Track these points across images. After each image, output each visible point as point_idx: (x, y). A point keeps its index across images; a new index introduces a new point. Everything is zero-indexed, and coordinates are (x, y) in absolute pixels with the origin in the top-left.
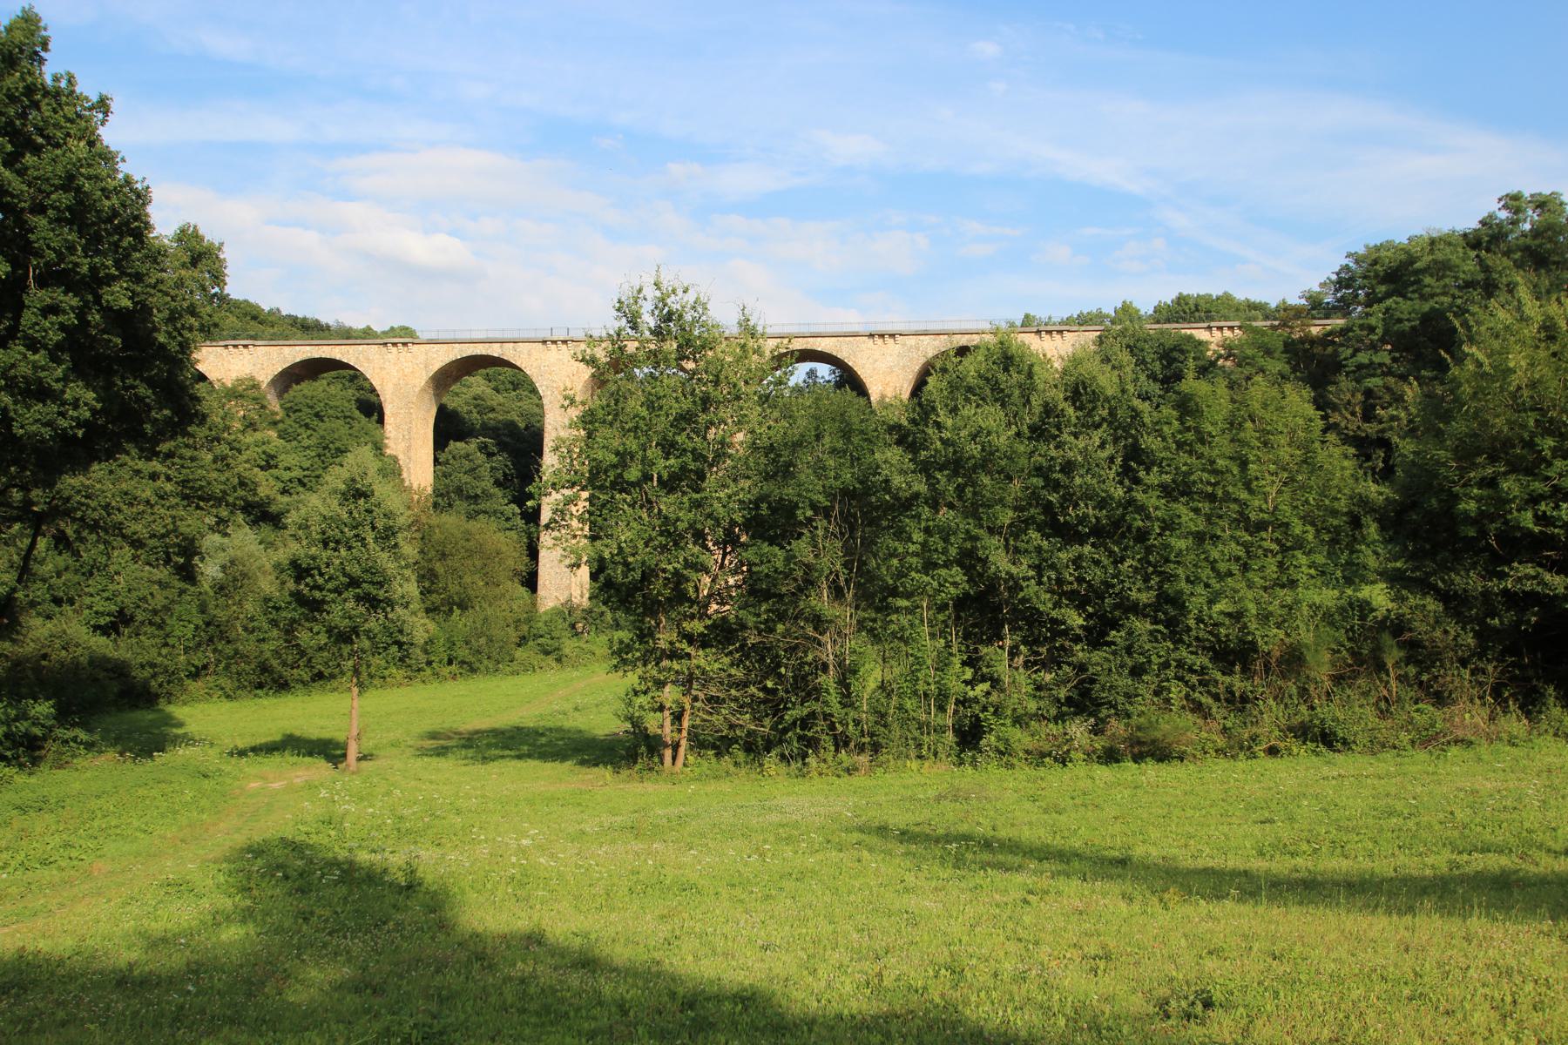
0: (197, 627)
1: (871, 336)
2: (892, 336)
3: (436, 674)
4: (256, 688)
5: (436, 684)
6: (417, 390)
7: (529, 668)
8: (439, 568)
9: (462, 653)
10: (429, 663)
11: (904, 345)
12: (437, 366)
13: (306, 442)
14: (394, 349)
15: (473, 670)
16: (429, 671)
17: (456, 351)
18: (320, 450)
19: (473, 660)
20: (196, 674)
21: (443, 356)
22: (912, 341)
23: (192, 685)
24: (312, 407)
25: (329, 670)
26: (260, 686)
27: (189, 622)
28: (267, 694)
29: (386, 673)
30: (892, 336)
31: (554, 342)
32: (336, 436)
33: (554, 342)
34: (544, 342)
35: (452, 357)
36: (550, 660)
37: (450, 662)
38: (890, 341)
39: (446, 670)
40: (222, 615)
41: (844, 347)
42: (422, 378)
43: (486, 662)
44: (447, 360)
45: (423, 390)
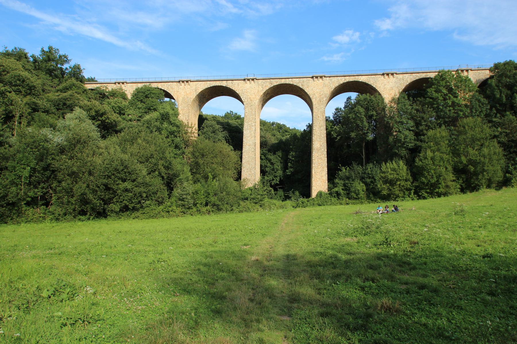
0: (34, 170)
1: (383, 74)
2: (392, 74)
3: (199, 211)
4: (82, 215)
5: (199, 216)
6: (192, 100)
7: (248, 210)
8: (201, 161)
9: (213, 199)
10: (195, 205)
11: (397, 78)
12: (200, 90)
13: (140, 106)
14: (183, 84)
15: (219, 209)
16: (195, 209)
18: (147, 110)
19: (220, 203)
20: (33, 203)
21: (202, 86)
22: (400, 76)
23: (30, 211)
24: (144, 93)
25: (133, 205)
26: (83, 213)
27: (28, 166)
28: (89, 219)
29: (170, 209)
30: (392, 74)
31: (249, 80)
32: (154, 104)
33: (249, 80)
34: (244, 80)
35: (206, 87)
36: (257, 206)
37: (206, 205)
39: (204, 209)
40: (56, 164)
42: (193, 95)
43: (226, 206)
45: (194, 100)
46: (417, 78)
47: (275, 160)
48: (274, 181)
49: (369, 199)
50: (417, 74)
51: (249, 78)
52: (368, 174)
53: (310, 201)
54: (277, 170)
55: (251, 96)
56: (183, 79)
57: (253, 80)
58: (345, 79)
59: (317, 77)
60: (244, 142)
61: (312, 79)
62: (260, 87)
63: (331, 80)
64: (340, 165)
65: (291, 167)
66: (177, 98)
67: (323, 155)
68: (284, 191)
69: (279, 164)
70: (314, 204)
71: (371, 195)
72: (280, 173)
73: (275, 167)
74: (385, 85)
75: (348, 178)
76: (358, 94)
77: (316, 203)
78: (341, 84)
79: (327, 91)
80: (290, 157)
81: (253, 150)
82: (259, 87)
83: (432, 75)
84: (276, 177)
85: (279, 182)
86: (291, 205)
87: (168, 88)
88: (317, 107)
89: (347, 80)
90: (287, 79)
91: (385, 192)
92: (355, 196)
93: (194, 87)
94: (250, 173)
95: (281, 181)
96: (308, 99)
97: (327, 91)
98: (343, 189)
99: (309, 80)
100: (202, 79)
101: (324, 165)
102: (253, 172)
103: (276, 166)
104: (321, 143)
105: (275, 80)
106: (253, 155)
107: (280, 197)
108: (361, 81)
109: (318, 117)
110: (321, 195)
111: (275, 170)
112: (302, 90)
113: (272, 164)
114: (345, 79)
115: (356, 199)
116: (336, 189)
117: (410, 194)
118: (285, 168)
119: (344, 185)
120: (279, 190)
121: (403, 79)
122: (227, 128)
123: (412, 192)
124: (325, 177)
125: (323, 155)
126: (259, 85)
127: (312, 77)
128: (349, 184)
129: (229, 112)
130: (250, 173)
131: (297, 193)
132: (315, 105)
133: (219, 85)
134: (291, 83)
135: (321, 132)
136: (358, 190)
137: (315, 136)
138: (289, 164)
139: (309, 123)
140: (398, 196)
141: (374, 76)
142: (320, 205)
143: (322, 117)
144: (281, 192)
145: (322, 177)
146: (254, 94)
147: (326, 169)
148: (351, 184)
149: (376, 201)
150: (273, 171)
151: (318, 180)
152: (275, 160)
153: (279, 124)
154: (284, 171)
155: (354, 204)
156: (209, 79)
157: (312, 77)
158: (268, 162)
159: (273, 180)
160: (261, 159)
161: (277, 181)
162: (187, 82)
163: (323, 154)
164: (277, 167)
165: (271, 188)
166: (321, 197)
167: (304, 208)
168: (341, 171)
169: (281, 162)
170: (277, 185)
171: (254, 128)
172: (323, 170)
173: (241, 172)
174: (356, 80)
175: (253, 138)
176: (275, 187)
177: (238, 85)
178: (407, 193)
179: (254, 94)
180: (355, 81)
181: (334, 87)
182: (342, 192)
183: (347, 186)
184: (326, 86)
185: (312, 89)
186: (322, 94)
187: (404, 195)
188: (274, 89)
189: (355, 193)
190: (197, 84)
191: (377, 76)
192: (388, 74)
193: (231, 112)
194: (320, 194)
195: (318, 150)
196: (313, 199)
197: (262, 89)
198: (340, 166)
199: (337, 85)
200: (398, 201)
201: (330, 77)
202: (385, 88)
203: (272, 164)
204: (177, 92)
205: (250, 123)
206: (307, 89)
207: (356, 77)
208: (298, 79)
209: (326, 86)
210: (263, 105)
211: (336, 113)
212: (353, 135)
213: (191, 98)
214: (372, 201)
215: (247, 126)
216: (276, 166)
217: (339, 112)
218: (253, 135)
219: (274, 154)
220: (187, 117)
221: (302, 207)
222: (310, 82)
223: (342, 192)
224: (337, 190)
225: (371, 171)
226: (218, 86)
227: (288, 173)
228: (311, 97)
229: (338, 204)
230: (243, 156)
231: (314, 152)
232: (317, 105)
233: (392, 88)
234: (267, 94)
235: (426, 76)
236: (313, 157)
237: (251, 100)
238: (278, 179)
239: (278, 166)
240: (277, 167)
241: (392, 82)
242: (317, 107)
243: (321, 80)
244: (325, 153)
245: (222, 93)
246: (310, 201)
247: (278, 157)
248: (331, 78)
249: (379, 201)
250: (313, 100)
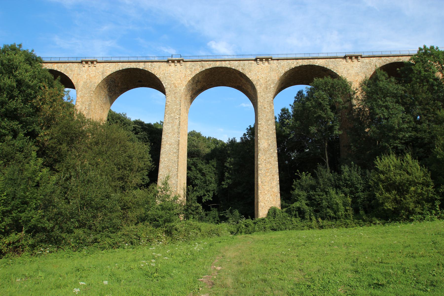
2: (357, 57)
6: (96, 85)
11: (363, 62)
12: (109, 73)
14: (86, 66)
22: (367, 60)
30: (357, 57)
34: (168, 62)
35: (117, 69)
36: (160, 233)
38: (355, 60)
41: (330, 63)
44: (114, 70)
46: (388, 62)
47: (207, 171)
48: (206, 197)
49: (358, 219)
50: (387, 58)
51: (174, 59)
52: (346, 180)
53: (259, 223)
54: (211, 183)
55: (175, 82)
56: (87, 59)
57: (179, 61)
58: (298, 63)
59: (261, 60)
60: (163, 140)
61: (255, 63)
62: (188, 70)
63: (279, 63)
64: (298, 171)
65: (228, 178)
66: (77, 82)
67: (273, 158)
68: (219, 211)
69: (212, 175)
70: (265, 228)
71: (362, 212)
72: (213, 186)
73: (207, 179)
74: (348, 70)
75: (313, 188)
77: (269, 225)
78: (293, 69)
79: (275, 76)
80: (227, 165)
81: (175, 151)
82: (186, 71)
83: (406, 59)
84: (208, 191)
85: (212, 198)
86: (228, 230)
87: (66, 70)
88: (262, 96)
89: (301, 64)
90: (223, 62)
91: (389, 206)
92: (332, 215)
93: (101, 70)
95: (214, 196)
96: (250, 90)
97: (275, 76)
98: (307, 204)
99: (251, 63)
100: (114, 59)
101: (274, 172)
103: (208, 178)
104: (270, 141)
105: (208, 62)
106: (176, 158)
107: (214, 218)
108: (317, 65)
109: (265, 108)
110: (275, 214)
111: (208, 183)
112: (242, 76)
113: (203, 175)
114: (298, 63)
115: (333, 218)
116: (297, 204)
117: (433, 207)
118: (221, 179)
119: (309, 198)
120: (212, 209)
121: (370, 64)
122: (147, 128)
123: (437, 203)
124: (276, 189)
125: (273, 158)
126: (186, 68)
127: (256, 60)
128: (317, 196)
129: (159, 123)
131: (237, 212)
132: (260, 93)
133: (135, 67)
134: (229, 66)
135: (269, 127)
136: (337, 204)
137: (261, 133)
138: (226, 174)
139: (250, 126)
140: (412, 213)
141: (334, 60)
142: (274, 230)
143: (269, 108)
144: (214, 212)
145: (272, 188)
146: (180, 78)
147: (277, 177)
148: (319, 195)
149: (371, 222)
150: (204, 184)
151: (266, 192)
152: (207, 171)
153: (215, 139)
154: (220, 184)
155: (330, 227)
156: (122, 60)
157: (256, 60)
158: (198, 172)
159: (205, 195)
160: (189, 168)
161: (209, 197)
162: (92, 62)
163: (272, 157)
164: (210, 179)
165: (198, 204)
166: (274, 217)
167: (250, 235)
168: (299, 178)
169: (215, 173)
170: (209, 202)
171: (177, 122)
172: (273, 179)
175: (176, 135)
176: (206, 207)
178: (427, 206)
179: (180, 78)
180: (309, 65)
181: (283, 72)
182: (306, 208)
183: (314, 199)
184: (273, 70)
185: (256, 74)
186: (269, 81)
187: (423, 210)
188: (206, 74)
189: (332, 209)
190: (105, 66)
191: (337, 59)
192: (351, 57)
193: (161, 122)
194: (272, 212)
195: (265, 151)
196: (263, 219)
197: (190, 73)
198: (297, 173)
199: (287, 69)
200: (412, 220)
201: (278, 60)
202: (348, 74)
203: (203, 175)
204: (78, 74)
205: (172, 115)
206: (249, 73)
207: (311, 60)
208: (237, 62)
209: (273, 70)
210: (193, 98)
211: (282, 115)
212: (313, 129)
213: (95, 83)
214: (364, 221)
215: (169, 118)
216: (208, 178)
217: (285, 113)
218: (176, 130)
219: (208, 163)
220: (87, 106)
221: (246, 233)
222: (253, 65)
223: (306, 208)
224: (298, 205)
225: (349, 176)
227: (224, 186)
229: (306, 227)
231: (260, 154)
232: (263, 94)
233: (357, 74)
234: (198, 81)
235: (398, 60)
236: (259, 160)
237: (175, 87)
238: (211, 194)
239: (212, 177)
240: (210, 179)
241: (356, 67)
242: (262, 96)
243: (266, 63)
244: (275, 155)
245: (139, 81)
246: (259, 223)
247: (212, 167)
248: (279, 61)
249: (378, 222)
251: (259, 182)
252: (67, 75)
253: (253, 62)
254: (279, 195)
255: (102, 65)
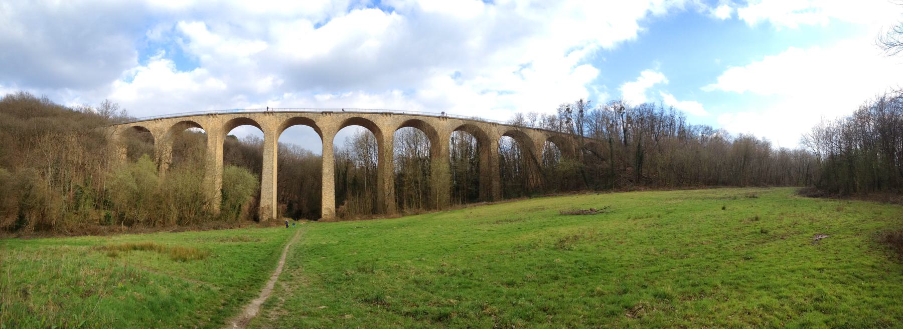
12: (226, 122)
17: (233, 117)
22: (396, 116)
42: (220, 126)
62: (278, 119)
76: (367, 129)
94: (268, 192)
96: (319, 131)
102: (271, 191)
126: (276, 117)
130: (268, 192)
133: (243, 117)
137: (325, 163)
145: (331, 197)
147: (333, 191)
173: (261, 191)
174: (360, 117)
175: (271, 163)
177: (259, 117)
207: (360, 114)
208: (312, 114)
218: (271, 159)
222: (321, 117)
226: (242, 118)
228: (321, 129)
230: (263, 178)
232: (326, 137)
237: (270, 130)
243: (329, 116)
250: (323, 133)
251: (323, 194)
252: (199, 124)
253: (321, 114)
254: (334, 201)
255: (221, 116)
